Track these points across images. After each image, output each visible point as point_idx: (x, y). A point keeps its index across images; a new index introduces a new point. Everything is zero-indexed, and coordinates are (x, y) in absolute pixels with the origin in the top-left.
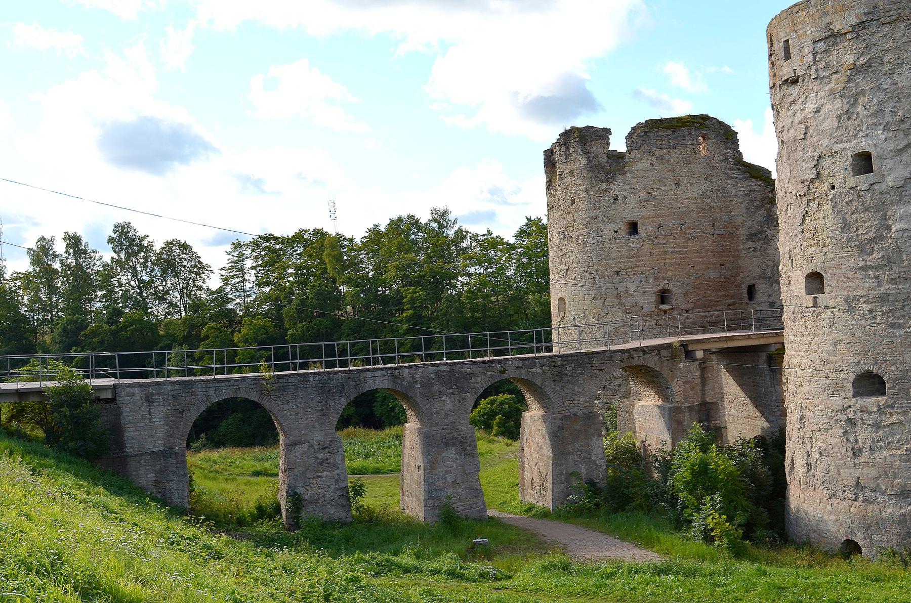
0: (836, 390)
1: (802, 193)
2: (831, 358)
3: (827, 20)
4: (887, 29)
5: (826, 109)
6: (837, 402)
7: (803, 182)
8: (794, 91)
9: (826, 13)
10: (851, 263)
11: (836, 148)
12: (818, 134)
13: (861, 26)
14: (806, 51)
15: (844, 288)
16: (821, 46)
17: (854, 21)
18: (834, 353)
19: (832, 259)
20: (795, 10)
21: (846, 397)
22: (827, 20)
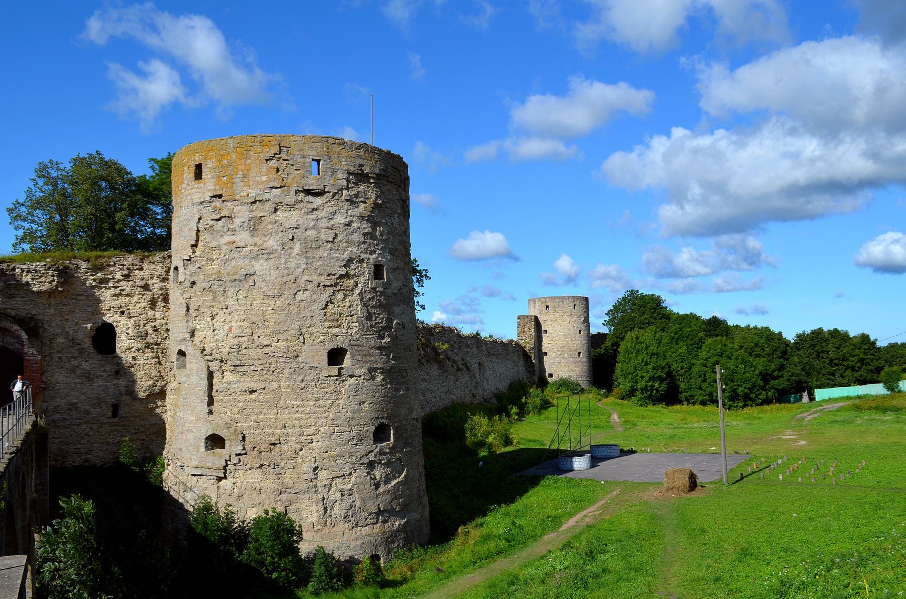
0: (361, 439)
1: (328, 283)
2: (356, 415)
4: (389, 187)
5: (355, 225)
6: (361, 449)
7: (329, 275)
8: (318, 201)
10: (372, 343)
11: (363, 256)
12: (347, 242)
14: (340, 176)
15: (366, 362)
18: (360, 411)
19: (358, 339)
20: (331, 141)
21: (368, 444)
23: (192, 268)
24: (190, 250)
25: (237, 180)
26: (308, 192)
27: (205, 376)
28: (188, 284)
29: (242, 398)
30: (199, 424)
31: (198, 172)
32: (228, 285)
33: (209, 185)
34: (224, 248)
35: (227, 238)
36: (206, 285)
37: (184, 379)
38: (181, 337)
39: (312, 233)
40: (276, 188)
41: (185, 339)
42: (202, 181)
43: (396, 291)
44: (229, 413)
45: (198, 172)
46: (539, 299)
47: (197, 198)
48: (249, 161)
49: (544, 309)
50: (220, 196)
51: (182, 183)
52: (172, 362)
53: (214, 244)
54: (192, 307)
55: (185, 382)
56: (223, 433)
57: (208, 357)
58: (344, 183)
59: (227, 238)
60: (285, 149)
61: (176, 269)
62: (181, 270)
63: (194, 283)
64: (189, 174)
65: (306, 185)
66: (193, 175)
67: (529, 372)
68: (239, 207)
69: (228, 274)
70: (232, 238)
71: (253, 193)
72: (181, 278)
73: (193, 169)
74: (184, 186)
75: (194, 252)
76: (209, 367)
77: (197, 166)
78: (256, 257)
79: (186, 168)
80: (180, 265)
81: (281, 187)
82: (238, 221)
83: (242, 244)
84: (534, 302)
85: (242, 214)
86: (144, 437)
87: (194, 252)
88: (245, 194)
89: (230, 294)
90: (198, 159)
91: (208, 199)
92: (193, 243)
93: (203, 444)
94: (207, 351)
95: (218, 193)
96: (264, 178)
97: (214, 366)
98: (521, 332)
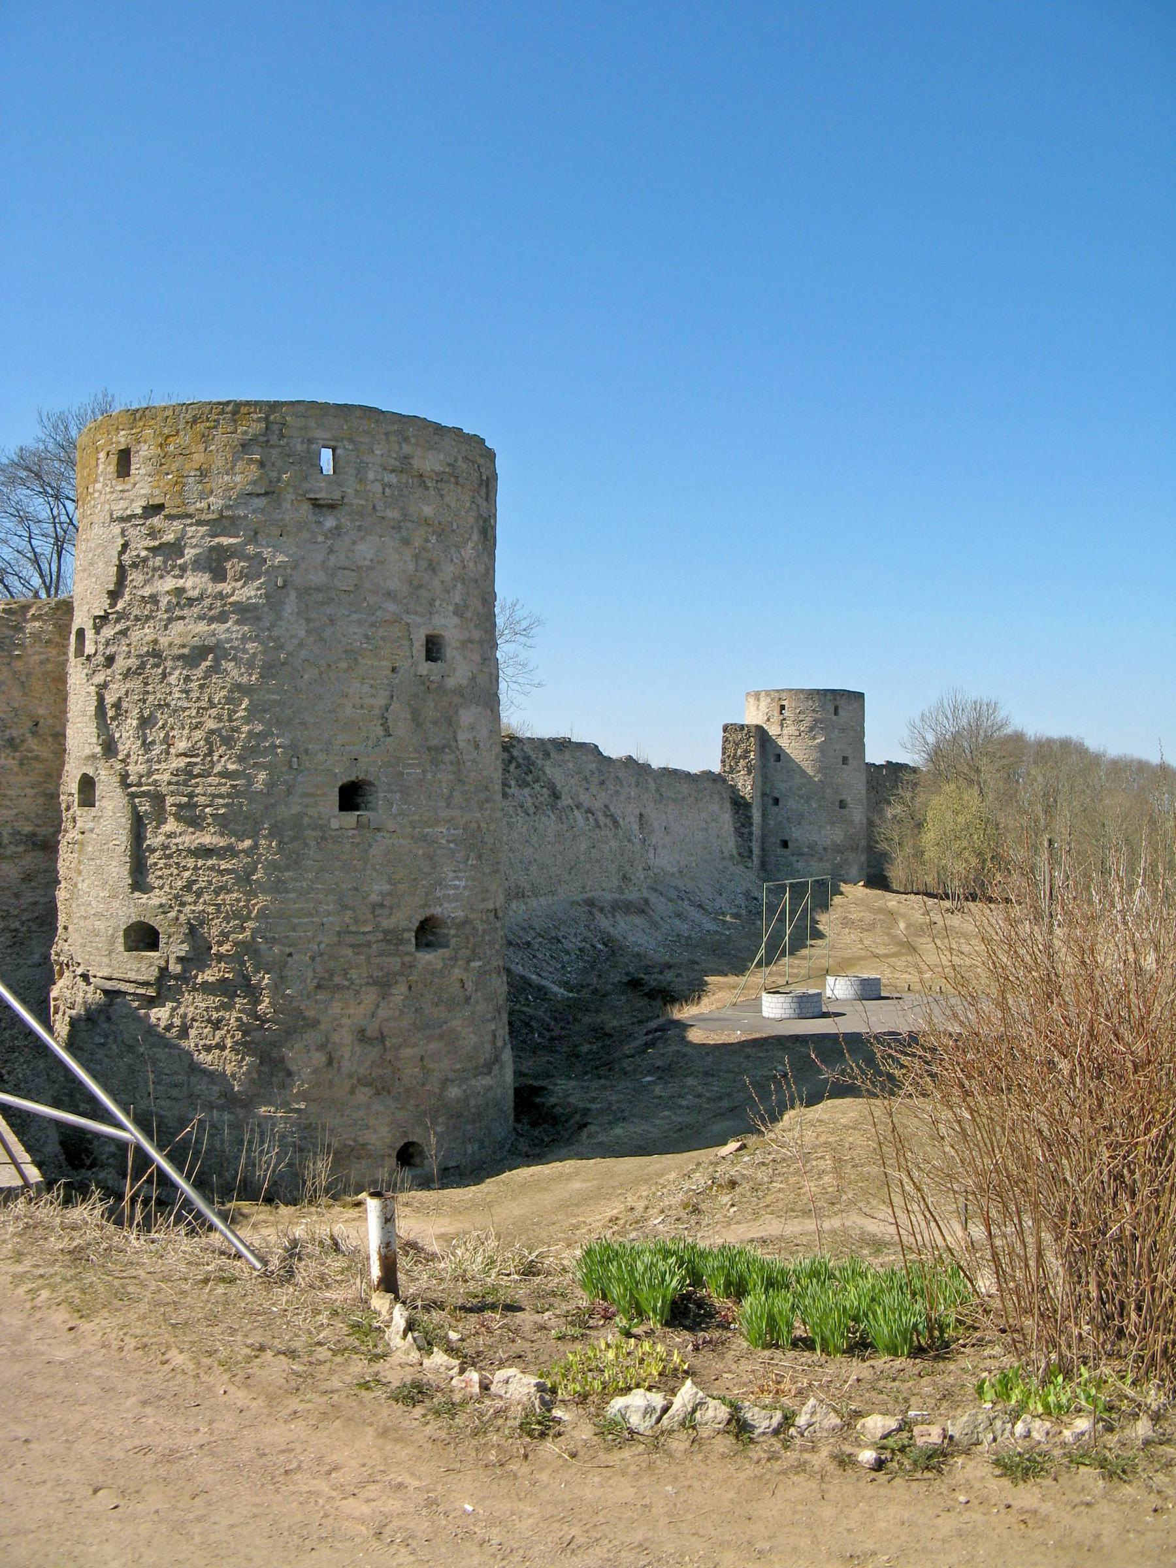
3: (406, 449)
9: (406, 440)
13: (440, 478)
16: (392, 478)
17: (437, 468)
22: (406, 449)
23: (108, 632)
25: (191, 480)
26: (316, 504)
27: (125, 822)
28: (100, 659)
29: (191, 862)
30: (116, 904)
31: (124, 460)
32: (169, 664)
33: (142, 486)
34: (164, 601)
35: (170, 583)
36: (133, 662)
37: (91, 825)
38: (87, 752)
40: (258, 495)
41: (93, 756)
42: (131, 480)
43: (465, 682)
44: (167, 888)
45: (124, 460)
46: (768, 693)
47: (119, 509)
48: (213, 447)
49: (776, 713)
50: (159, 508)
51: (96, 481)
52: (71, 794)
53: (147, 591)
54: (110, 699)
55: (92, 830)
56: (157, 922)
57: (133, 789)
58: (377, 487)
59: (170, 583)
60: (275, 427)
61: (81, 633)
62: (90, 634)
63: (110, 660)
64: (106, 467)
65: (310, 491)
66: (112, 468)
67: (741, 835)
68: (194, 528)
69: (170, 645)
70: (180, 583)
72: (89, 649)
73: (114, 459)
74: (99, 486)
75: (112, 605)
76: (134, 807)
77: (121, 451)
78: (222, 618)
79: (102, 455)
80: (88, 626)
81: (266, 494)
82: (190, 553)
83: (195, 594)
84: (757, 696)
85: (197, 539)
86: (17, 924)
87: (112, 605)
89: (172, 679)
90: (122, 439)
91: (139, 511)
92: (111, 587)
93: (121, 940)
94: (132, 779)
95: (157, 501)
97: (145, 807)
98: (730, 757)
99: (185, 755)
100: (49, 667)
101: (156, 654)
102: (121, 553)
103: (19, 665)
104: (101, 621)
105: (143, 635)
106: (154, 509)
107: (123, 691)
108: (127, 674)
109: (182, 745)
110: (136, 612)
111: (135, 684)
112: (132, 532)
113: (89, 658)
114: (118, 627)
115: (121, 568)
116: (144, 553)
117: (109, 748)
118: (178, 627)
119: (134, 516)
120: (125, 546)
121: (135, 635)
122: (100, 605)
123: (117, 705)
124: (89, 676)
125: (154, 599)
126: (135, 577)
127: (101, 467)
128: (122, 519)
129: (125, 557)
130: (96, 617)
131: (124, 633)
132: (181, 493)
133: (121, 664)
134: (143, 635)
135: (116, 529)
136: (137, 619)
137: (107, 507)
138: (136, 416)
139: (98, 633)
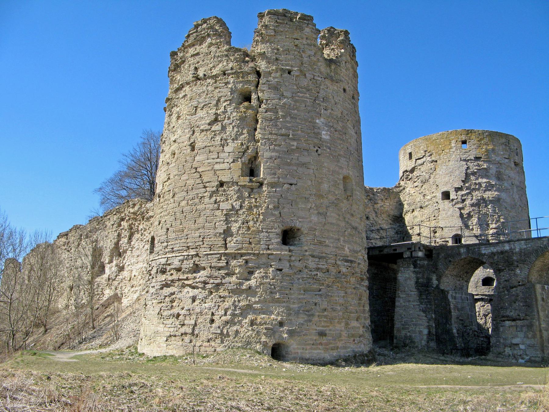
23: (460, 193)
24: (462, 184)
28: (459, 200)
34: (484, 185)
35: (485, 180)
39: (518, 184)
47: (463, 157)
53: (477, 182)
63: (463, 201)
71: (498, 159)
72: (452, 197)
79: (453, 142)
82: (491, 171)
88: (493, 159)
89: (489, 207)
90: (463, 138)
91: (473, 158)
92: (464, 179)
96: (502, 153)
99: (494, 228)
100: (382, 208)
101: (483, 199)
102: (466, 170)
103: (376, 206)
104: (457, 190)
105: (477, 195)
106: (477, 159)
107: (471, 210)
108: (472, 205)
109: (494, 226)
110: (473, 187)
111: (476, 209)
112: (470, 164)
113: (453, 200)
114: (468, 191)
115: (466, 174)
116: (475, 171)
117: (467, 227)
118: (487, 193)
119: (471, 160)
120: (468, 168)
121: (474, 194)
122: (458, 184)
123: (469, 214)
124: (453, 206)
125: (480, 184)
126: (472, 178)
127: (453, 145)
128: (465, 160)
129: (468, 171)
130: (455, 188)
131: (470, 193)
132: (487, 155)
133: (468, 202)
134: (477, 195)
135: (465, 163)
136: (473, 189)
137: (458, 156)
138: (469, 132)
139: (457, 192)
